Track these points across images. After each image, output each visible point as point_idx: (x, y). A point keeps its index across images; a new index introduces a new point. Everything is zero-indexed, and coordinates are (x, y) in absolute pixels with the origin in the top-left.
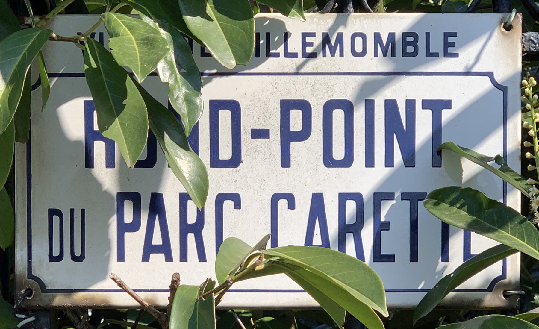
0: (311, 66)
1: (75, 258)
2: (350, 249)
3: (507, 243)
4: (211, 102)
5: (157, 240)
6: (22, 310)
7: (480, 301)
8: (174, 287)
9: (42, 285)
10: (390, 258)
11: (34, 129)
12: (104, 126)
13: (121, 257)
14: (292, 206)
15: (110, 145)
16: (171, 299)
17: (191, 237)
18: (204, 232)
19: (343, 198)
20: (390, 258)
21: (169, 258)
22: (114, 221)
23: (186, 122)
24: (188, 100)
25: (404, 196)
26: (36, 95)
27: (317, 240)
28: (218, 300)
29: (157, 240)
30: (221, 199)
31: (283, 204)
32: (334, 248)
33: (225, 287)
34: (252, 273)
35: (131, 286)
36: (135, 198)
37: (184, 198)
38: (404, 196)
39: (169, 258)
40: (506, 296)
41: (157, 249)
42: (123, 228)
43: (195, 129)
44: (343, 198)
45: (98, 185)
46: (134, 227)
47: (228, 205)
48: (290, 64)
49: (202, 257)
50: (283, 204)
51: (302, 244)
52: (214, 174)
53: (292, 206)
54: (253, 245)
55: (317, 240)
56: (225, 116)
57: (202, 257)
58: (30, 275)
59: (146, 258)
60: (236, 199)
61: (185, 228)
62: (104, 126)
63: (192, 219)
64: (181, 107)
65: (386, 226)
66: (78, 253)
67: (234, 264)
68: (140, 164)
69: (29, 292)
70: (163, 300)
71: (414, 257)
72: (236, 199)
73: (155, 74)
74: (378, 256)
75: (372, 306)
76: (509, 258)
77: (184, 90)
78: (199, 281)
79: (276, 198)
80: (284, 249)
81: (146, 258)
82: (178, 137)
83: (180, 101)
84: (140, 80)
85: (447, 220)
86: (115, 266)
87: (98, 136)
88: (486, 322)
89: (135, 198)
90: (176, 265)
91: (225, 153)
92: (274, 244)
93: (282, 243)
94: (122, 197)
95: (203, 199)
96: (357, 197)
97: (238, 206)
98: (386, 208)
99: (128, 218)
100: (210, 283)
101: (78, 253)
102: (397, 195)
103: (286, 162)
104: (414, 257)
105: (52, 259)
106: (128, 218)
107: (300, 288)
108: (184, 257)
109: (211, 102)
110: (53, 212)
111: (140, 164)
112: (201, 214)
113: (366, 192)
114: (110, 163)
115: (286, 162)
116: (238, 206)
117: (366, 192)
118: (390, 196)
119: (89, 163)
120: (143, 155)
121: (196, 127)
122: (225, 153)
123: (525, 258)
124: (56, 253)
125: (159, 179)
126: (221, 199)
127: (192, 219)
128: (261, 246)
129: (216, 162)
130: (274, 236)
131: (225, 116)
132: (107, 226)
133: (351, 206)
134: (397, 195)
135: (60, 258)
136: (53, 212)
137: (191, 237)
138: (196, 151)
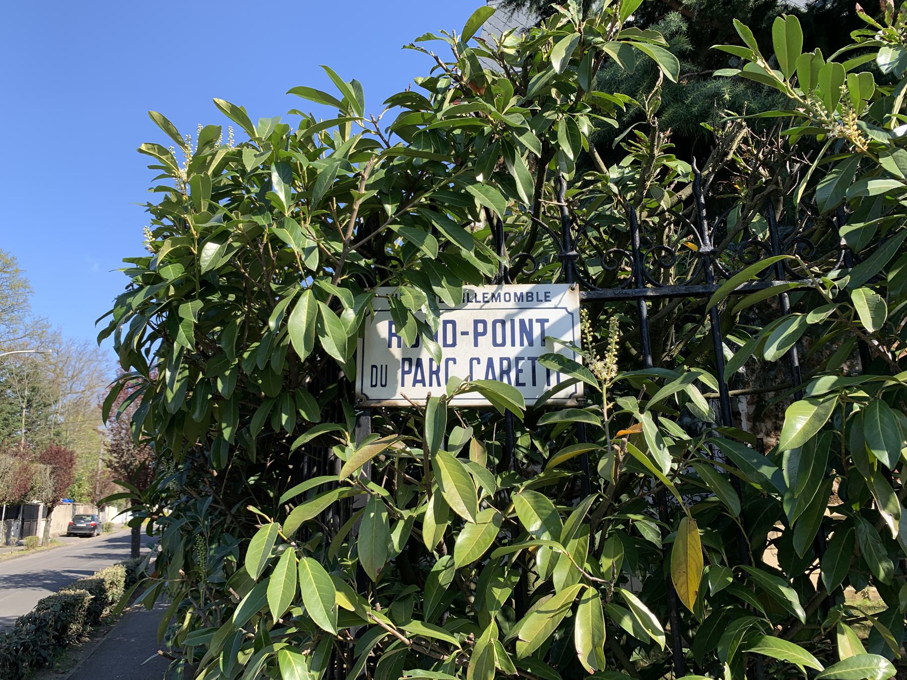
0: (487, 306)
1: (382, 386)
2: (505, 381)
3: (577, 377)
4: (444, 321)
5: (419, 377)
6: (357, 408)
7: (565, 403)
8: (428, 398)
9: (367, 397)
10: (524, 385)
11: (366, 332)
12: (398, 330)
13: (403, 385)
14: (479, 363)
15: (399, 339)
16: (427, 403)
17: (434, 376)
18: (440, 374)
19: (502, 359)
20: (524, 385)
21: (424, 385)
22: (400, 371)
23: (433, 329)
24: (434, 320)
25: (529, 359)
26: (368, 318)
27: (490, 377)
28: (448, 403)
29: (419, 377)
30: (447, 360)
31: (475, 362)
32: (498, 380)
33: (451, 397)
34: (464, 391)
35: (409, 398)
36: (410, 360)
37: (431, 360)
38: (529, 359)
39: (424, 385)
40: (577, 401)
41: (419, 382)
42: (404, 373)
43: (437, 332)
44: (502, 359)
45: (393, 356)
46: (409, 372)
47: (451, 363)
48: (478, 305)
49: (439, 385)
50: (475, 362)
51: (484, 379)
52: (444, 350)
53: (479, 363)
54: (463, 379)
55: (490, 377)
56: (450, 326)
57: (439, 385)
58: (362, 393)
59: (414, 385)
60: (454, 360)
61: (432, 373)
62: (398, 330)
63: (434, 369)
64: (431, 323)
65: (521, 371)
66: (384, 383)
67: (455, 388)
68: (413, 346)
69: (361, 400)
70: (423, 403)
71: (534, 384)
72: (454, 360)
73: (420, 310)
74: (518, 384)
75: (517, 405)
76: (578, 384)
77: (433, 316)
78: (439, 395)
79: (472, 360)
80: (475, 382)
81: (414, 385)
82: (429, 335)
83: (431, 320)
84: (414, 312)
85: (549, 367)
86: (400, 389)
87: (395, 335)
88: (569, 411)
89: (410, 360)
90: (428, 389)
91: (450, 341)
92: (471, 380)
93: (475, 379)
94: (404, 360)
95: (440, 361)
96: (508, 359)
97: (455, 363)
98: (521, 363)
99: (407, 368)
100: (444, 396)
101: (384, 383)
102: (526, 358)
103: (476, 345)
104: (534, 384)
105: (372, 386)
106: (407, 368)
107: (484, 397)
108: (431, 385)
109: (444, 321)
110: (373, 366)
111: (413, 346)
112: (438, 367)
113: (512, 357)
114: (399, 346)
115: (476, 345)
116: (455, 363)
117: (512, 357)
118: (523, 359)
119: (390, 346)
120: (414, 343)
121: (437, 332)
122: (450, 341)
123: (585, 384)
124: (374, 383)
125: (420, 353)
126: (447, 360)
127: (434, 369)
128: (466, 380)
129: (445, 345)
130: (471, 377)
131: (450, 326)
132: (396, 374)
133: (505, 363)
134: (526, 358)
135: (375, 386)
136: (373, 366)
137: (434, 376)
138: (437, 341)
